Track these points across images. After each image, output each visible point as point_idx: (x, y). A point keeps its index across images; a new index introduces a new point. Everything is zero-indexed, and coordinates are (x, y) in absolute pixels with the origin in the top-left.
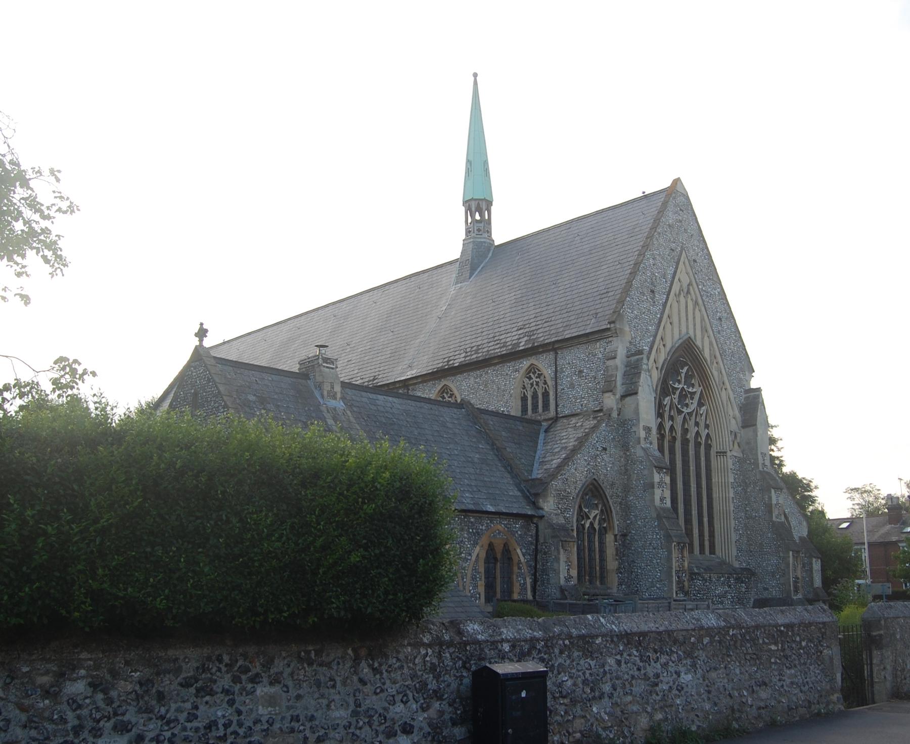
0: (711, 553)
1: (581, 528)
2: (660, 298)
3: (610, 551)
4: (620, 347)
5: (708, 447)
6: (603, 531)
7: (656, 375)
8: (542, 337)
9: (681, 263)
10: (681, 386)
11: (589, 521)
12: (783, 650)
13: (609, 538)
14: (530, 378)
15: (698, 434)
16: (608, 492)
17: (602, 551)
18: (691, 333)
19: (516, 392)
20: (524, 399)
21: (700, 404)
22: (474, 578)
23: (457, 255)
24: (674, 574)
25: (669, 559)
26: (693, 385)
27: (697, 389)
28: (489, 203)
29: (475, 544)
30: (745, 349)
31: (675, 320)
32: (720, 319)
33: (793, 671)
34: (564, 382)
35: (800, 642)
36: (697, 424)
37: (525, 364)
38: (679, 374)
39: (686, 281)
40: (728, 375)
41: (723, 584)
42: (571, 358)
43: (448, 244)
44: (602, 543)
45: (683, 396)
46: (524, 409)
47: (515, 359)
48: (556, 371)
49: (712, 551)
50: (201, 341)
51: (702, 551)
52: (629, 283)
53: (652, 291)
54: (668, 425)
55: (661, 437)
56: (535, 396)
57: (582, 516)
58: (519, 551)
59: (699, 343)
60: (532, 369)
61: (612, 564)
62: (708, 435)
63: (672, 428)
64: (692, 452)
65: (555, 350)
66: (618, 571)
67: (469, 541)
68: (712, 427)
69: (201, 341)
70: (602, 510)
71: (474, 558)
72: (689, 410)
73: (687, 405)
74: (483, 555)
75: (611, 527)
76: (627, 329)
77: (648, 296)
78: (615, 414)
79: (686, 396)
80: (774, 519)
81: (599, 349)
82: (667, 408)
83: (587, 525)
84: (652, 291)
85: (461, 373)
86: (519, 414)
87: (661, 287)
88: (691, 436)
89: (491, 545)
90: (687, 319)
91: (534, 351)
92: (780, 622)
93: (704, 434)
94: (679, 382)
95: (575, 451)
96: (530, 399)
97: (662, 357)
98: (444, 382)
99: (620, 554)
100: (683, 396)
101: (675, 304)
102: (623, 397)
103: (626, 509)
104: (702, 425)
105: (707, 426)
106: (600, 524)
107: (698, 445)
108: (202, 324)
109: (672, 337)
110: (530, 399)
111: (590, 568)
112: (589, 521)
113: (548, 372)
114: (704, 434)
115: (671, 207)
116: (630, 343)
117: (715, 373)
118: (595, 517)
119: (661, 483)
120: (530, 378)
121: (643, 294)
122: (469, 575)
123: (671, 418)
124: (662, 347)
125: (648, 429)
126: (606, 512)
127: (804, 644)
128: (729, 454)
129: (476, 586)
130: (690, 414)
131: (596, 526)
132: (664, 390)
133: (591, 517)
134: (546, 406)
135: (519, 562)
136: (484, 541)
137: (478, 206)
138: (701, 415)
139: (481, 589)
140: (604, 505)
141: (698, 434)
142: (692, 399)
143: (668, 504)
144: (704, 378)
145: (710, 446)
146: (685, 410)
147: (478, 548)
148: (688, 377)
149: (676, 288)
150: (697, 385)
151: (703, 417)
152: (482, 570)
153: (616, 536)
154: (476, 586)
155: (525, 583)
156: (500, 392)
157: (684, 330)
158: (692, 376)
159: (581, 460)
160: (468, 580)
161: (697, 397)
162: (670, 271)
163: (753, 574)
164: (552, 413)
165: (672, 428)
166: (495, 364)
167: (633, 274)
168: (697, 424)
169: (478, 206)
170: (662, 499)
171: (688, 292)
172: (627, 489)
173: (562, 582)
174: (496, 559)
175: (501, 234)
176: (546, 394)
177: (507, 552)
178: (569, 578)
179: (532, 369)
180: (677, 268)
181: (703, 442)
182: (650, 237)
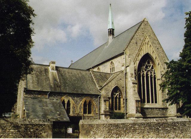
0: (155, 103)
2: (139, 44)
5: (155, 78)
6: (119, 99)
11: (115, 96)
13: (122, 100)
15: (151, 75)
16: (121, 89)
18: (149, 53)
20: (111, 69)
21: (152, 68)
22: (80, 108)
27: (151, 65)
29: (81, 101)
32: (158, 48)
36: (151, 73)
37: (111, 61)
44: (120, 101)
46: (111, 72)
49: (156, 102)
51: (152, 102)
53: (136, 43)
56: (112, 68)
58: (94, 102)
59: (152, 55)
60: (112, 62)
61: (122, 105)
62: (155, 76)
63: (143, 74)
67: (79, 100)
68: (156, 74)
70: (120, 94)
72: (149, 69)
74: (83, 103)
79: (148, 67)
83: (115, 96)
84: (136, 43)
88: (149, 76)
89: (85, 101)
100: (147, 67)
106: (119, 96)
109: (142, 54)
112: (115, 96)
115: (142, 24)
118: (117, 95)
126: (121, 94)
130: (149, 71)
131: (118, 97)
133: (117, 94)
135: (94, 105)
138: (153, 71)
139: (82, 111)
141: (151, 75)
142: (150, 67)
144: (153, 62)
147: (81, 102)
150: (151, 64)
151: (153, 71)
154: (81, 110)
158: (150, 62)
159: (113, 82)
160: (78, 109)
161: (151, 66)
168: (151, 73)
176: (114, 68)
181: (153, 77)
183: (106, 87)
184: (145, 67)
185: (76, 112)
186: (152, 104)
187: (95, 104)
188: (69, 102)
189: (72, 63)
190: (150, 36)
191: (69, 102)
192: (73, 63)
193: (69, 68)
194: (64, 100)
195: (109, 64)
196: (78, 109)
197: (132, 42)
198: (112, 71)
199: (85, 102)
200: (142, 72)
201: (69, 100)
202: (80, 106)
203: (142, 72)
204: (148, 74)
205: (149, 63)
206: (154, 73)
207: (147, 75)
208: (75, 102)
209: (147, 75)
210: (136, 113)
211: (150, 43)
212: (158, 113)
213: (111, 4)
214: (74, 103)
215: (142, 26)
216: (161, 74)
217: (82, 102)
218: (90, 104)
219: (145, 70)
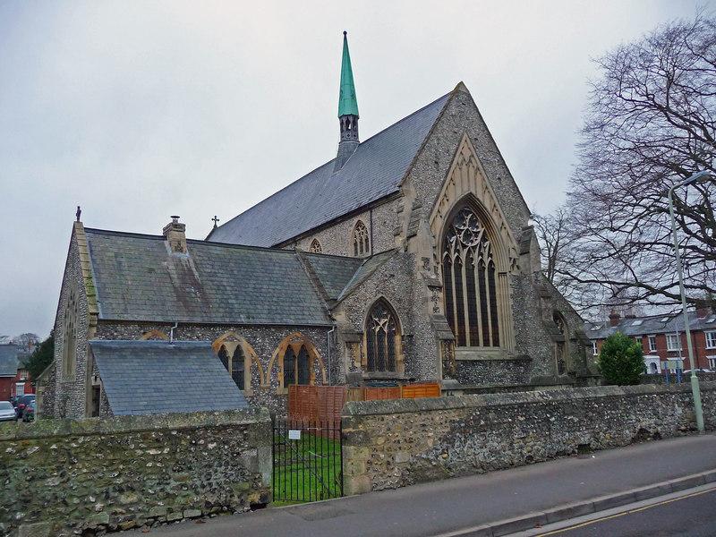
1: (370, 334)
3: (398, 347)
4: (406, 203)
5: (492, 270)
6: (391, 335)
7: (440, 224)
8: (365, 201)
9: (463, 141)
10: (466, 228)
12: (173, 452)
13: (398, 338)
14: (358, 230)
15: (482, 261)
16: (395, 305)
17: (391, 347)
18: (474, 192)
19: (350, 240)
20: (356, 244)
21: (484, 239)
22: (273, 371)
23: (334, 156)
24: (441, 362)
25: (438, 352)
26: (477, 227)
27: (481, 230)
28: (356, 117)
30: (522, 198)
31: (457, 180)
32: (499, 179)
33: (185, 474)
34: (376, 230)
35: (205, 445)
37: (355, 220)
38: (463, 219)
39: (467, 154)
40: (507, 218)
41: (503, 367)
42: (379, 213)
43: (327, 147)
44: (391, 342)
45: (468, 235)
46: (356, 253)
47: (350, 218)
48: (371, 224)
49: (496, 343)
50: (78, 219)
51: (486, 343)
52: (416, 159)
53: (436, 163)
54: (453, 257)
55: (447, 265)
56: (361, 243)
57: (370, 322)
58: (315, 350)
60: (359, 224)
61: (400, 357)
62: (491, 262)
64: (476, 275)
65: (371, 210)
66: (405, 360)
69: (78, 219)
71: (274, 357)
72: (473, 245)
73: (472, 242)
74: (283, 354)
75: (399, 330)
76: (412, 189)
77: (432, 166)
78: (402, 251)
80: (544, 319)
81: (394, 205)
82: (453, 244)
83: (377, 330)
85: (322, 230)
86: (353, 256)
87: (444, 160)
88: (476, 262)
90: (469, 181)
91: (361, 210)
92: (170, 426)
93: (487, 261)
94: (465, 225)
95: (366, 278)
96: (359, 244)
97: (446, 209)
98: (314, 237)
99: (404, 348)
100: (468, 235)
101: (458, 171)
102: (409, 238)
103: (411, 317)
104: (486, 254)
105: (490, 255)
106: (389, 327)
107: (482, 270)
108: (79, 207)
109: (455, 195)
110: (359, 244)
111: (379, 358)
113: (367, 225)
114: (487, 261)
115: (454, 103)
116: (416, 200)
117: (495, 217)
118: (384, 325)
119: (434, 298)
120: (358, 230)
121: (428, 165)
122: (270, 369)
123: (458, 251)
124: (445, 200)
125: (426, 260)
126: (394, 321)
127: (211, 446)
128: (508, 274)
129: (276, 376)
130: (474, 247)
131: (386, 330)
132: (450, 230)
133: (381, 324)
134: (367, 250)
136: (284, 344)
137: (349, 122)
138: (485, 248)
139: (281, 379)
140: (392, 315)
141: (482, 261)
143: (442, 312)
144: (487, 222)
145: (494, 270)
146: (470, 245)
147: (278, 349)
148: (473, 223)
149: (458, 159)
151: (487, 249)
152: (281, 364)
153: (403, 337)
154: (276, 376)
155: (321, 373)
156: (339, 243)
157: (466, 189)
158: (477, 220)
159: (371, 284)
160: (268, 372)
161: (480, 235)
162: (453, 148)
163: (531, 360)
164: (370, 254)
165: (458, 258)
166: (339, 223)
167: (420, 152)
169: (349, 122)
170: (435, 309)
171: (470, 161)
172: (411, 302)
173: (348, 372)
174: (294, 356)
175: (364, 134)
177: (304, 349)
178: (353, 368)
179: (359, 224)
180: (459, 145)
182: (435, 125)
183: (350, 301)
184: (462, 235)
185: (263, 382)
186: (487, 348)
187: (318, 356)
188: (238, 351)
189: (215, 226)
190: (476, 139)
191: (238, 351)
192: (219, 225)
193: (207, 242)
194: (223, 347)
195: (352, 228)
196: (268, 372)
197: (422, 158)
198: (362, 251)
199: (289, 349)
200: (452, 250)
201: (238, 347)
202: (275, 364)
203: (452, 250)
204: (472, 259)
205: (473, 223)
206: (490, 255)
207: (469, 260)
208: (256, 351)
209: (469, 260)
210: (444, 377)
211: (476, 163)
212: (503, 376)
213: (345, 33)
214: (255, 354)
215: (453, 110)
216: (511, 258)
217: (279, 352)
218: (305, 353)
219: (464, 246)
